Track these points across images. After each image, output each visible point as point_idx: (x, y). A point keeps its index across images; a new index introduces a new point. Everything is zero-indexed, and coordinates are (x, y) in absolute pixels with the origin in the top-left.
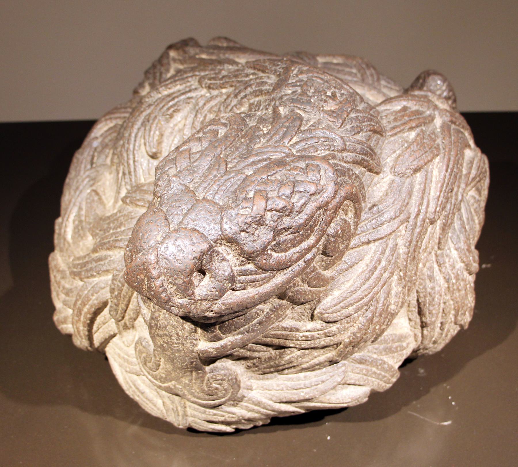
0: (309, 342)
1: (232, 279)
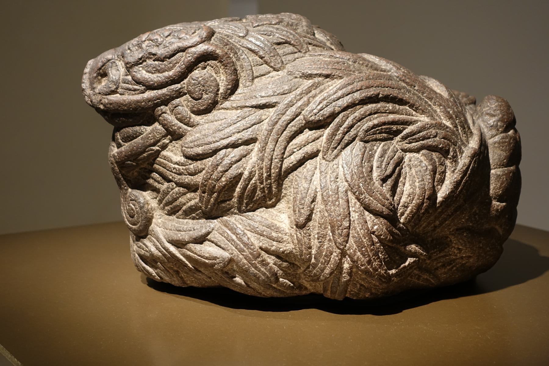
0: (179, 177)
1: (117, 83)
